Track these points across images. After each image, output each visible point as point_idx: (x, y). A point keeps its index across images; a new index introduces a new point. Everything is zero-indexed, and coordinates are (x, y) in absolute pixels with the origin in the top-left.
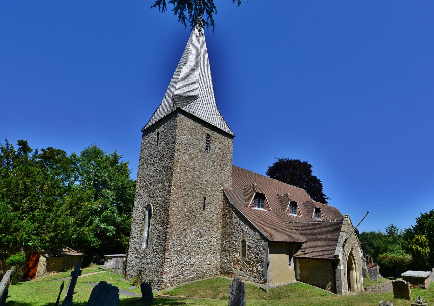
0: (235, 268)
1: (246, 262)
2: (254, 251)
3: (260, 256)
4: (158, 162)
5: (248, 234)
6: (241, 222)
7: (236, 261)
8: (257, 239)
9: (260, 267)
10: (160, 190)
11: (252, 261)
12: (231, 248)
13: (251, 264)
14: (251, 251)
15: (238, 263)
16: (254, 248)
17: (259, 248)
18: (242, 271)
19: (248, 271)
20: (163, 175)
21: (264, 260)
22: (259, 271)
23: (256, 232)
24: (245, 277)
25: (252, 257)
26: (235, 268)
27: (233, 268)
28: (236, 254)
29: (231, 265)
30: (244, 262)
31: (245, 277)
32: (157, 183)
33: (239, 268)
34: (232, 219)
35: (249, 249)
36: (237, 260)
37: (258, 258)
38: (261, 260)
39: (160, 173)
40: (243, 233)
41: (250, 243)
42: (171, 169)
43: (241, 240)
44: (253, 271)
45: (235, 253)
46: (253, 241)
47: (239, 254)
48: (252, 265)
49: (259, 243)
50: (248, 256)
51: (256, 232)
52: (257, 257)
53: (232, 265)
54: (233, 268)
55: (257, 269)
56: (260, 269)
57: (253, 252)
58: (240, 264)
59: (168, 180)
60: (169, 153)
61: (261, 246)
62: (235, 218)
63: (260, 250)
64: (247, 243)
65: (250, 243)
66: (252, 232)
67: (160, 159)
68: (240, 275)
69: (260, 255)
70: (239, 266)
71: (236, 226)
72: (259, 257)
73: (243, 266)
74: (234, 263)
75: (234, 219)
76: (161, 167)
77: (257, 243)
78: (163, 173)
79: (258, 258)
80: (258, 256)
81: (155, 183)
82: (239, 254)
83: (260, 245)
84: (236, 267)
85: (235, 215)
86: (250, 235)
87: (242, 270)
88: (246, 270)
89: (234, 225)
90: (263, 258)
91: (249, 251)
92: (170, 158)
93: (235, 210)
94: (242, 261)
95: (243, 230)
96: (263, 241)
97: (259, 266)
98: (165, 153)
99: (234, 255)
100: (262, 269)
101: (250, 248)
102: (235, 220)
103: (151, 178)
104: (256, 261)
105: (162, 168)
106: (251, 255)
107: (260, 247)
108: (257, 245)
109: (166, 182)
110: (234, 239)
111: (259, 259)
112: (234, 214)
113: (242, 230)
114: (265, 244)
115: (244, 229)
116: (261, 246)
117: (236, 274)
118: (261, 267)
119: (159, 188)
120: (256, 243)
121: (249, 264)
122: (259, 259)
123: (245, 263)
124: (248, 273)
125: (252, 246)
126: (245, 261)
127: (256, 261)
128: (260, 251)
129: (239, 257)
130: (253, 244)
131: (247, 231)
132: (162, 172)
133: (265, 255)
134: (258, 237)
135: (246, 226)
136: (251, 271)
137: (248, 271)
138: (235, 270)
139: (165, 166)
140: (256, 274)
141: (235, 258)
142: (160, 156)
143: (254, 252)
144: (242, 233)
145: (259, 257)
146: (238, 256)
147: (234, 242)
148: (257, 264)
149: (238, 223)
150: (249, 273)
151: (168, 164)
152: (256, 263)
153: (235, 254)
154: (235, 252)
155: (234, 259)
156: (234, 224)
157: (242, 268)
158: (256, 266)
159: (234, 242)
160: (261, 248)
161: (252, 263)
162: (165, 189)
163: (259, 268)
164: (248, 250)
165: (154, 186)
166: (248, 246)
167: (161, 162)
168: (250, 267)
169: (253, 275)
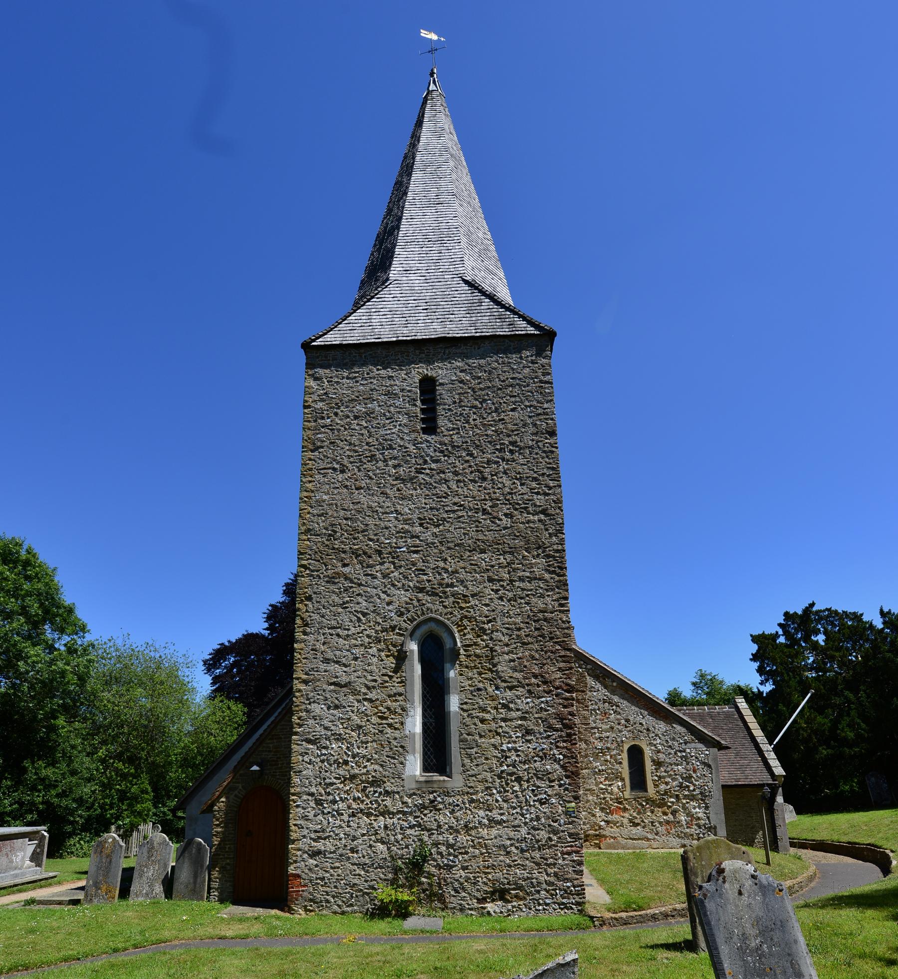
0: (607, 822)
1: (650, 802)
2: (675, 771)
3: (697, 783)
4: (458, 481)
5: (648, 730)
6: (616, 699)
7: (611, 802)
8: (681, 741)
9: (697, 810)
10: (496, 577)
11: (671, 797)
12: (586, 769)
13: (669, 804)
14: (665, 771)
15: (620, 808)
16: (675, 763)
17: (693, 764)
18: (639, 827)
19: (660, 823)
20: (505, 528)
21: (710, 792)
22: (699, 819)
23: (674, 725)
24: (648, 840)
25: (669, 787)
26: (607, 822)
27: (603, 823)
28: (610, 785)
29: (594, 815)
30: (644, 804)
31: (648, 840)
32: (470, 551)
33: (625, 821)
34: (583, 691)
35: (655, 769)
36: (617, 799)
37: (691, 788)
38: (701, 793)
39: (485, 519)
40: (628, 729)
41: (659, 751)
42: (547, 515)
43: (626, 747)
44: (678, 822)
45: (607, 782)
46: (670, 747)
47: (620, 784)
48: (670, 807)
49: (688, 751)
50: (656, 786)
51: (674, 725)
52: (688, 787)
53: (598, 815)
54: (603, 823)
55: (689, 814)
56: (699, 815)
57: (673, 773)
58: (629, 808)
59: (538, 548)
60: (521, 461)
61: (696, 758)
62: (593, 689)
63: (694, 767)
64: (648, 752)
65: (659, 751)
66: (661, 726)
67: (467, 471)
68: (631, 839)
69: (696, 781)
70: (627, 815)
71: (599, 709)
72: (694, 785)
73: (639, 813)
74: (602, 809)
75: (591, 691)
76: (485, 500)
77: (684, 751)
78: (500, 520)
79: (691, 788)
80: (692, 783)
81: (449, 548)
82: (620, 784)
83: (692, 756)
84: (615, 817)
85: (590, 681)
86: (653, 732)
87: (636, 825)
88: (652, 823)
89: (590, 708)
90: (707, 786)
91: (658, 774)
92: (535, 479)
93: (591, 669)
94: (635, 799)
95: (627, 721)
96: (701, 746)
97: (694, 808)
98: (497, 457)
99: (601, 786)
100: (705, 813)
101: (658, 764)
102: (595, 694)
103: (418, 529)
104: (685, 797)
105: (489, 503)
106: (667, 783)
107: (694, 762)
108: (681, 757)
109: (529, 553)
110: (600, 745)
111: (694, 790)
112: (588, 678)
113: (623, 722)
114: (707, 752)
115: (631, 718)
116: (696, 758)
117: (615, 838)
118: (700, 808)
119: (488, 570)
120: (680, 751)
121: (662, 804)
122: (694, 790)
123: (647, 804)
124: (660, 829)
125: (668, 760)
126: (648, 800)
127: (685, 797)
128: (695, 771)
129: (622, 792)
130: (670, 754)
131: (644, 723)
132: (494, 518)
133: (712, 781)
134: (684, 736)
135: (637, 709)
136: (668, 822)
137: (658, 825)
138: (611, 827)
139: (508, 500)
140: (688, 827)
141: (609, 796)
142: (467, 461)
143: (676, 775)
144: (626, 727)
145: (694, 785)
146: (619, 789)
147: (599, 753)
148: (687, 803)
149: (604, 703)
150: (664, 827)
151: (526, 497)
152: (684, 801)
153: (606, 785)
154: (606, 779)
155: (604, 798)
156: (592, 704)
157: (636, 818)
158: (684, 808)
159: (599, 753)
160: (698, 764)
161: (672, 802)
162: (528, 577)
163: (696, 813)
164: (654, 771)
165: (449, 559)
166: (653, 761)
167: (474, 481)
168: (665, 814)
169: (676, 832)
